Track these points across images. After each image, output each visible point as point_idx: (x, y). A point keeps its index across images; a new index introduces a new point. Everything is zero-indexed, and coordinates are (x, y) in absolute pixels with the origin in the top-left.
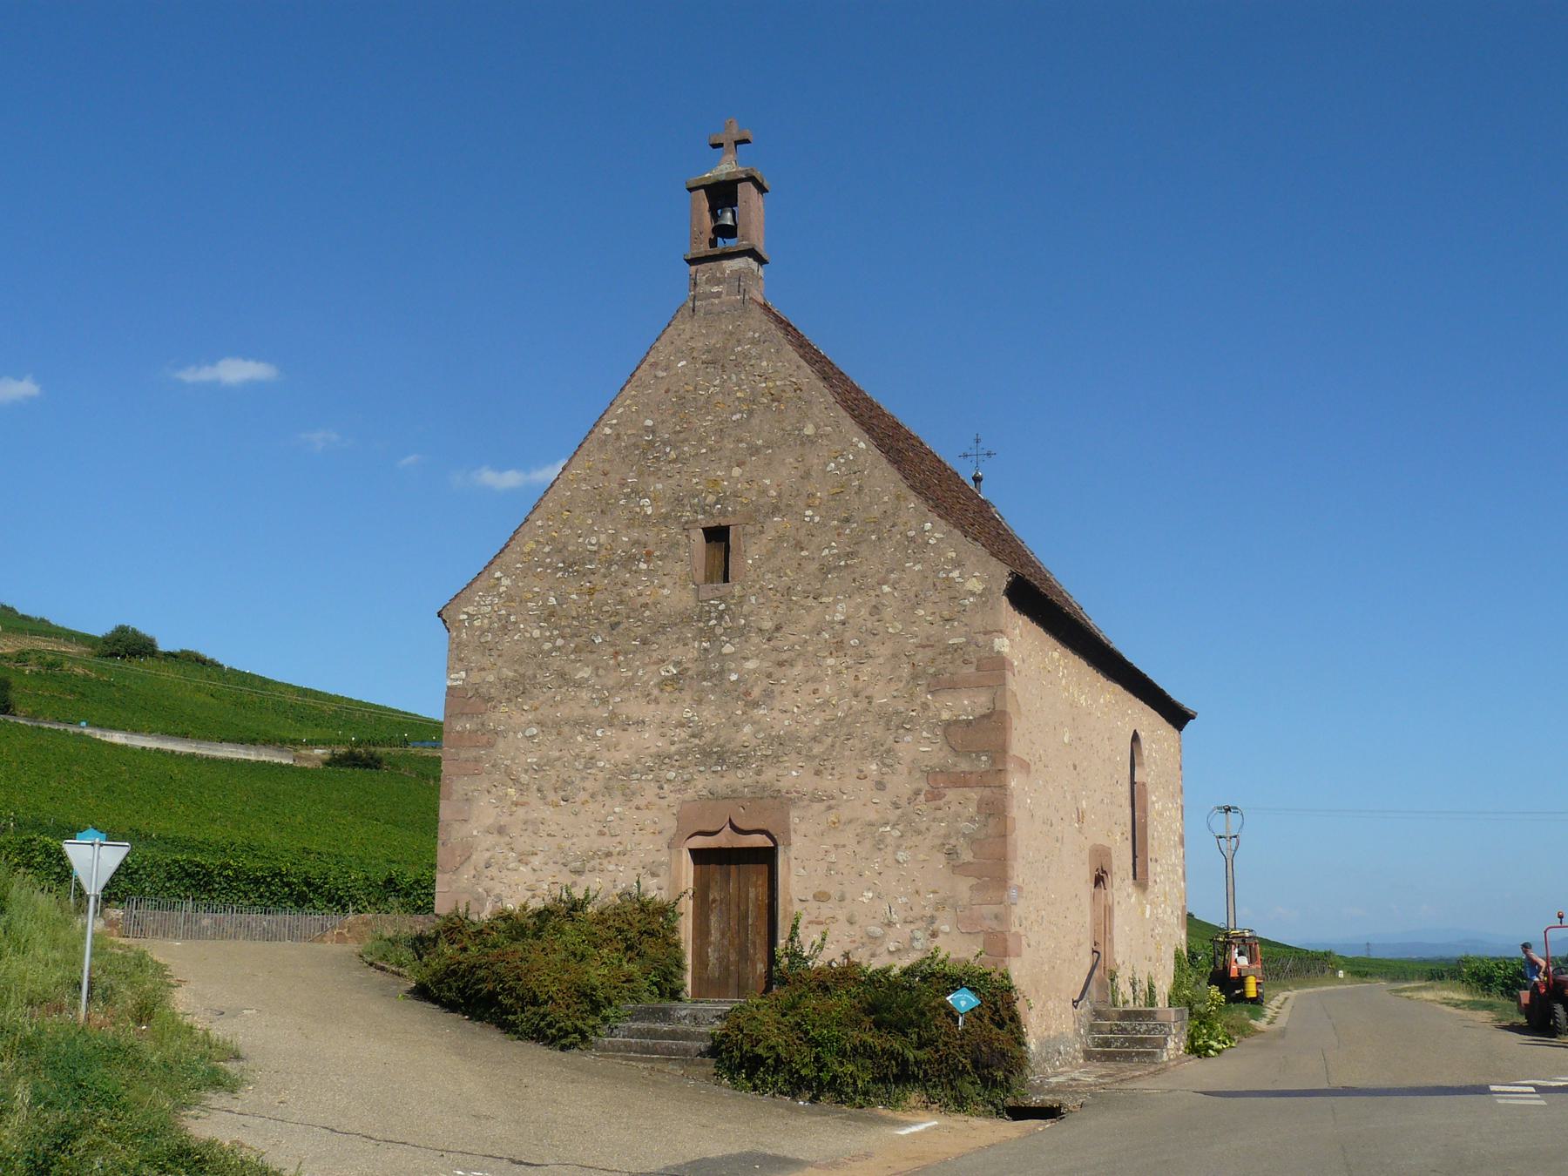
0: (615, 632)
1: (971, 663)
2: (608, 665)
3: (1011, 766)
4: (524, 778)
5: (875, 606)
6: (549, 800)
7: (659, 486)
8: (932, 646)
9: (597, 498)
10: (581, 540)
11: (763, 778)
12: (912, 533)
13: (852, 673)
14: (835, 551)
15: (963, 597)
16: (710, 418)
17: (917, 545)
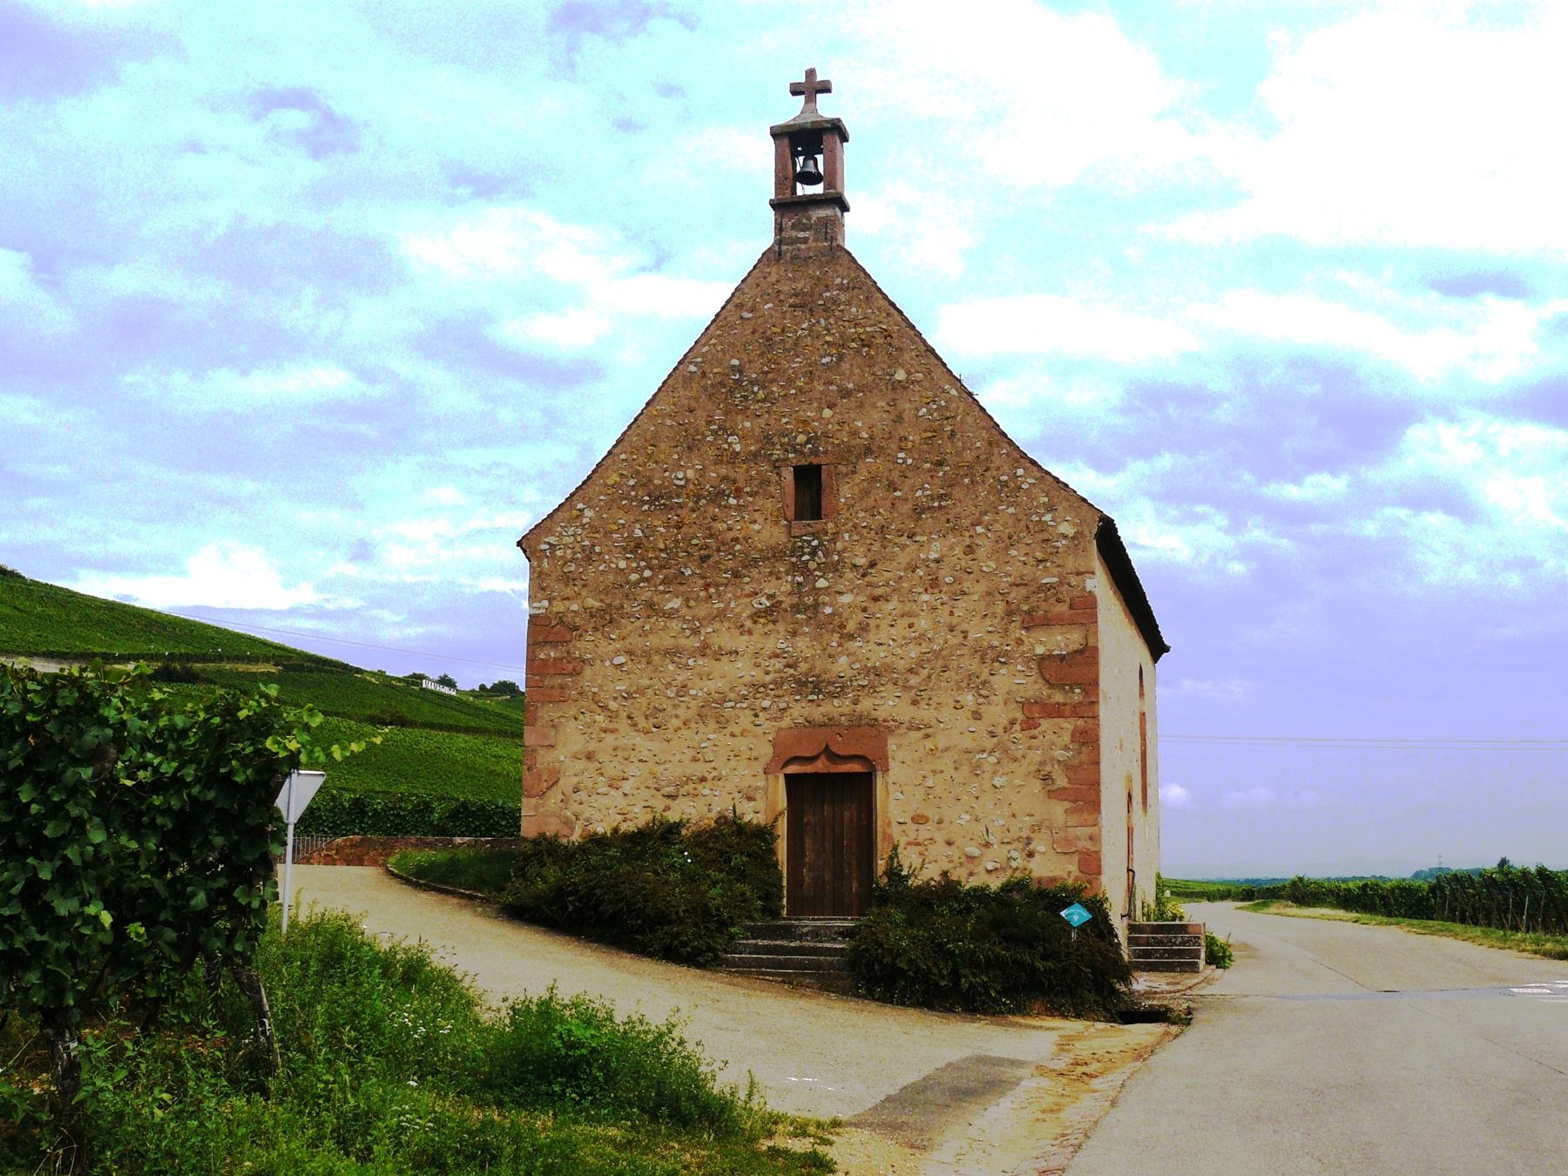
0: (705, 565)
2: (699, 596)
4: (613, 705)
5: (968, 546)
6: (640, 726)
7: (747, 424)
8: (1026, 585)
9: (684, 433)
10: (667, 474)
11: (859, 708)
12: (1004, 478)
13: (947, 609)
16: (799, 360)
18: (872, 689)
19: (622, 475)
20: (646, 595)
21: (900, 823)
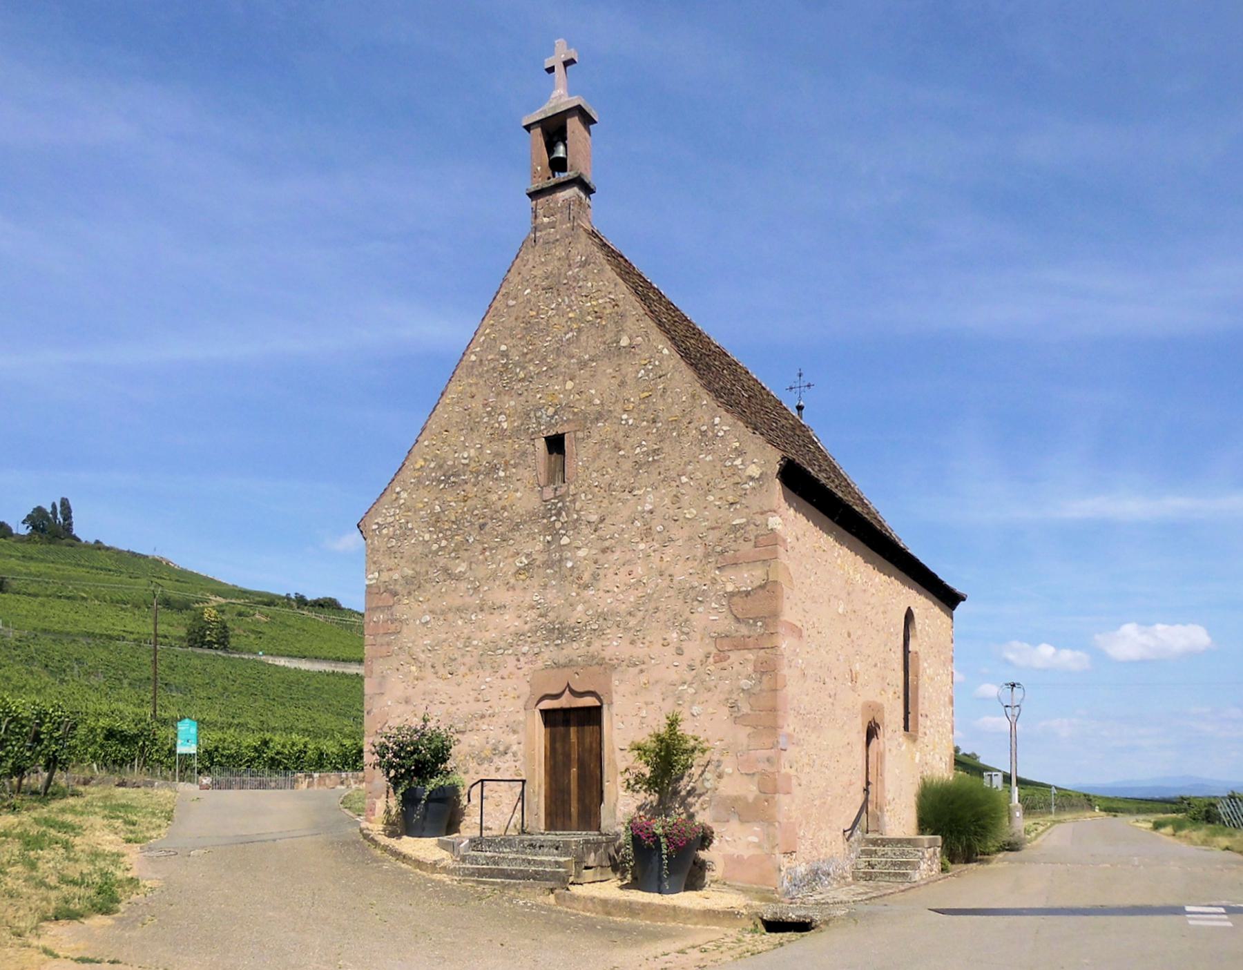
0: (482, 532)
1: (750, 540)
2: (478, 560)
3: (782, 630)
4: (422, 657)
5: (675, 496)
6: (440, 674)
7: (512, 403)
9: (468, 417)
10: (456, 455)
11: (592, 649)
12: (704, 428)
13: (658, 555)
14: (645, 449)
15: (744, 481)
16: (549, 338)
17: (706, 438)
18: (600, 632)
19: (425, 460)
20: (442, 562)
21: (622, 750)
